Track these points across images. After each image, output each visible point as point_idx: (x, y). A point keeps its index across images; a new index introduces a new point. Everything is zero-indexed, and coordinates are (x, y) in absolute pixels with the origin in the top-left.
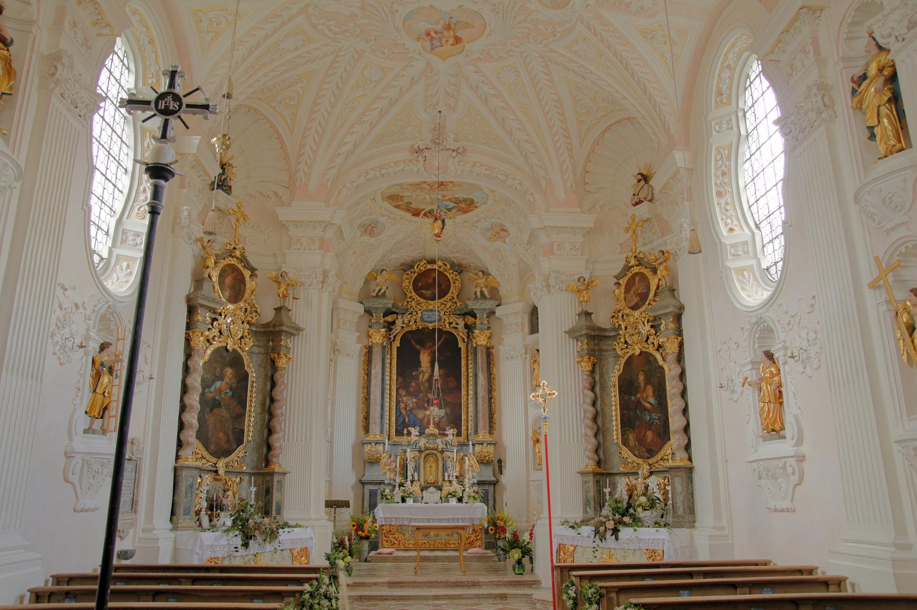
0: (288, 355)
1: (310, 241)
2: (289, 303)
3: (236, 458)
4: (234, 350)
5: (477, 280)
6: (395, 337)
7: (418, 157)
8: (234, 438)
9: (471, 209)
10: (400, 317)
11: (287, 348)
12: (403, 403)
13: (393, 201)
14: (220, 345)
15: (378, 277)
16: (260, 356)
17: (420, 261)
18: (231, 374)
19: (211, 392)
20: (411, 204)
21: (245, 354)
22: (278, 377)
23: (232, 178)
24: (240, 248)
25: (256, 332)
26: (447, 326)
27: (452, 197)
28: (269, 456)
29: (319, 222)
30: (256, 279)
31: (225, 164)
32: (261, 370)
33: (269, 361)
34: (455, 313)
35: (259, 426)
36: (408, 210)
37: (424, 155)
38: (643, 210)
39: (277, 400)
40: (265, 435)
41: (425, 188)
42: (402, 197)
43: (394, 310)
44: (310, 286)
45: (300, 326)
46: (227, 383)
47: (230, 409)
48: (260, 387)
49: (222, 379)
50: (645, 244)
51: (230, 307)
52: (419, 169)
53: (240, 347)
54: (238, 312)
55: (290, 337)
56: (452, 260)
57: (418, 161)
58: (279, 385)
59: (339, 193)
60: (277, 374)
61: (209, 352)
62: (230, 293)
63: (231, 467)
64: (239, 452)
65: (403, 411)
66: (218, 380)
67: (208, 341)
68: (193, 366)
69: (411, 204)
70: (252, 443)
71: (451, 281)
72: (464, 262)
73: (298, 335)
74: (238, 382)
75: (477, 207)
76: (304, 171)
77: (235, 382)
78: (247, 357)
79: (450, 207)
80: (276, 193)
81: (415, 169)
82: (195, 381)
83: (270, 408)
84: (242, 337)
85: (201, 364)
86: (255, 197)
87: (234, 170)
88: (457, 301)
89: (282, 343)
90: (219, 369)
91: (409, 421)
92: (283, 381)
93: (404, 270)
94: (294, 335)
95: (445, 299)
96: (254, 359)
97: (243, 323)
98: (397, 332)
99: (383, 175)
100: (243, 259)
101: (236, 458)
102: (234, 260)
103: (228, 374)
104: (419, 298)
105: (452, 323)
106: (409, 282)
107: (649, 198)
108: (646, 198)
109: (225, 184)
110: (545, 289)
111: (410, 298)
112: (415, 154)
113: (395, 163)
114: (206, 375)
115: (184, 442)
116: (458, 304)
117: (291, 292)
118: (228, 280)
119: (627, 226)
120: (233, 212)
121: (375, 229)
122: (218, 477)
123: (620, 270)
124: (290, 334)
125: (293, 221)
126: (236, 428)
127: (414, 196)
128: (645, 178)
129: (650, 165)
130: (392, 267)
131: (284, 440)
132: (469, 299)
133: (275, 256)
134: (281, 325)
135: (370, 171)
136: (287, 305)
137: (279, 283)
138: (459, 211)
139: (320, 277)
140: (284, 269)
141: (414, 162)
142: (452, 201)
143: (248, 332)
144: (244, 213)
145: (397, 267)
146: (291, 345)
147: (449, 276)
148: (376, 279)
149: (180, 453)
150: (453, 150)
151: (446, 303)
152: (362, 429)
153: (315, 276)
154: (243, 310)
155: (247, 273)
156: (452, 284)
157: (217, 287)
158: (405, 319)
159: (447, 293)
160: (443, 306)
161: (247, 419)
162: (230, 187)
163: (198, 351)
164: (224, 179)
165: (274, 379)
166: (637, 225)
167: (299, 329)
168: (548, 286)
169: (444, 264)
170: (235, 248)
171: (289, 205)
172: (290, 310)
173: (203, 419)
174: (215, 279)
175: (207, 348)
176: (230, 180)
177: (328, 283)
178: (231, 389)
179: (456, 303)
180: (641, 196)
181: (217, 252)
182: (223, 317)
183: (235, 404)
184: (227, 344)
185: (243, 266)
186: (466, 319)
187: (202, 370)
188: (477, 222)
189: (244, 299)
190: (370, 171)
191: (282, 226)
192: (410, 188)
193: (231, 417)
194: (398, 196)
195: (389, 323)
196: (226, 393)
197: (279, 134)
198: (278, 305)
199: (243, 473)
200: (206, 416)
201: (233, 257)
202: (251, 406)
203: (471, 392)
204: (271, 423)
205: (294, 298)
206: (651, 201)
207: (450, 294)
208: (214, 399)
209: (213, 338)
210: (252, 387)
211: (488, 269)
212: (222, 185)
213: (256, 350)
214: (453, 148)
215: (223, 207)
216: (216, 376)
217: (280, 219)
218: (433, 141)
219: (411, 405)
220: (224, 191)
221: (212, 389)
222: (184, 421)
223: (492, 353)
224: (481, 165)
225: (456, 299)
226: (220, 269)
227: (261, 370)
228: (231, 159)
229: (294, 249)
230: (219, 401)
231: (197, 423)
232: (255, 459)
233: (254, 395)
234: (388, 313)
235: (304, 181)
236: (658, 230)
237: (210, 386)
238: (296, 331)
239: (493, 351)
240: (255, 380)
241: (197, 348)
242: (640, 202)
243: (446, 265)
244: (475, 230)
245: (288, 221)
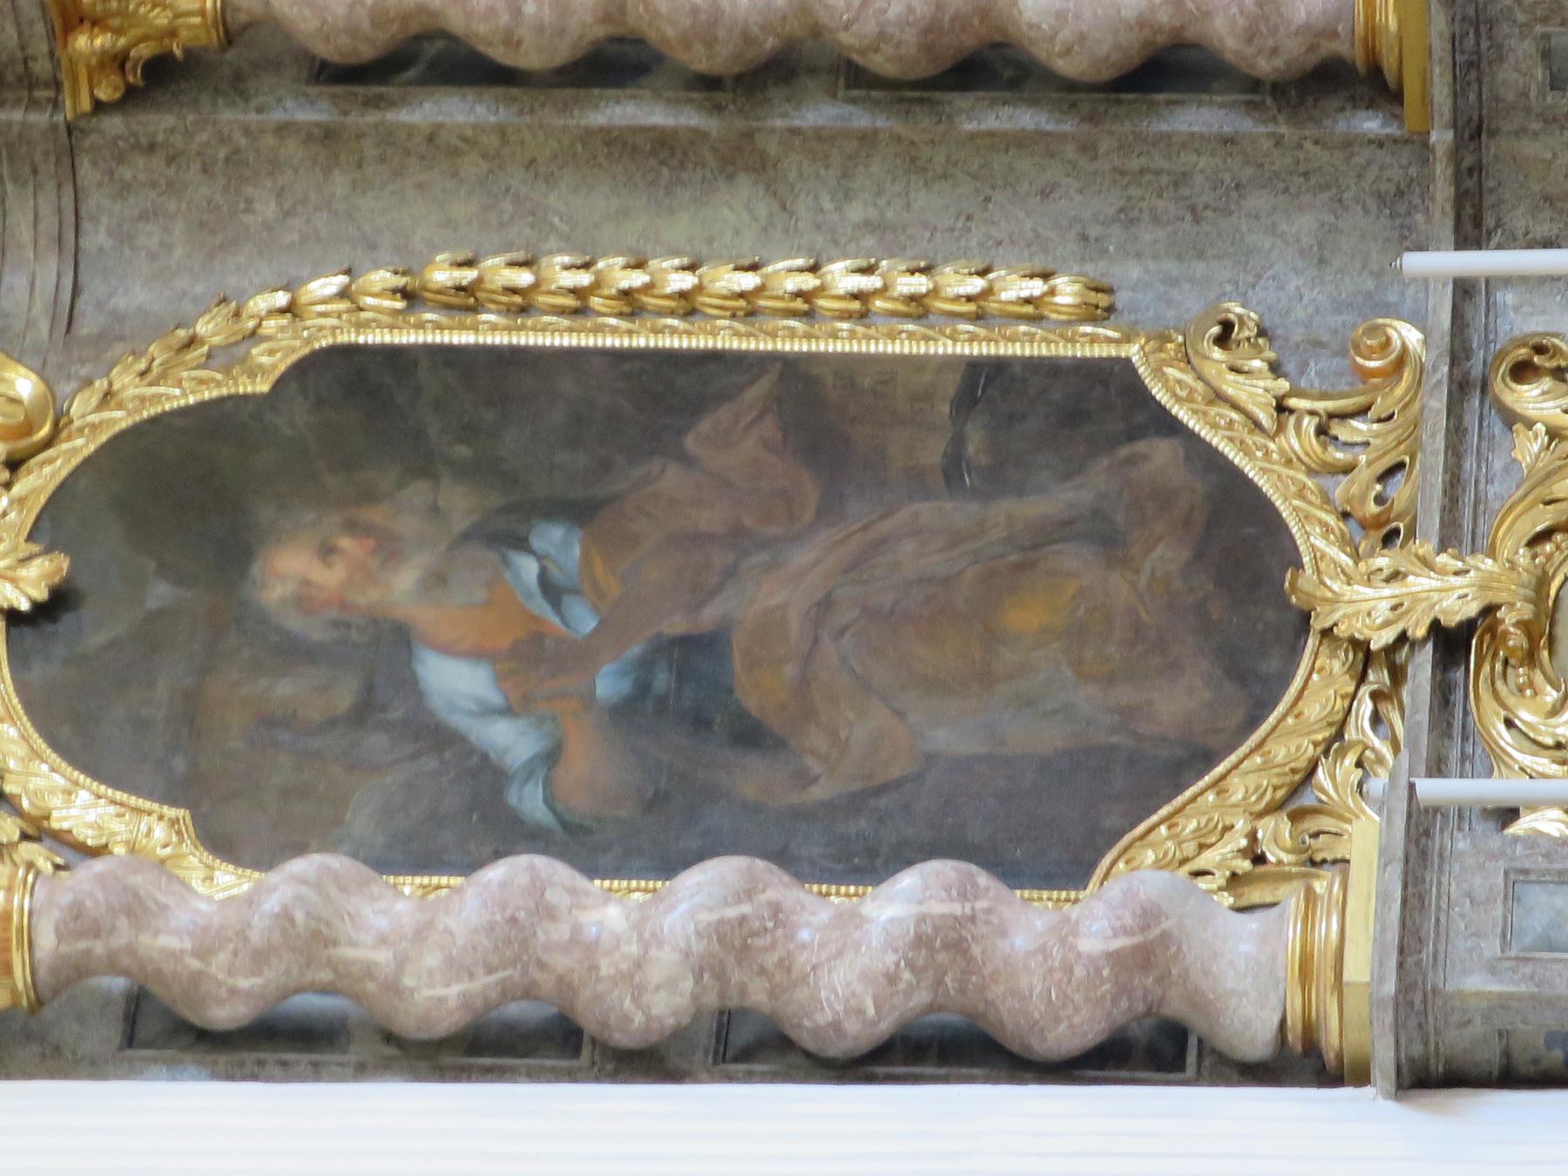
3: (1300, 439)
8: (1071, 472)
16: (97, 238)
18: (327, 552)
19: (552, 757)
21: (81, 407)
33: (160, 122)
35: (921, 199)
40: (1026, 118)
46: (437, 580)
47: (737, 537)
48: (462, 208)
63: (1400, 490)
66: (410, 686)
68: (260, 958)
70: (1127, 274)
74: (424, 465)
77: (417, 493)
78: (125, 381)
83: (708, 84)
85: (230, 881)
90: (284, 689)
101: (1300, 439)
103: (328, 577)
114: (361, 820)
115: (1122, 1012)
122: (1508, 618)
126: (953, 469)
161: (843, 342)
163: (78, 922)
165: (367, 53)
173: (861, 825)
183: (672, 479)
187: (299, 866)
193: (831, 508)
196: (551, 590)
199: (1459, 353)
200: (818, 793)
204: (881, 63)
208: (625, 712)
210: (466, 300)
216: (364, 712)
222: (885, 1027)
230: (645, 666)
231: (908, 880)
232: (1305, 224)
233: (563, 275)
240: (382, 278)
241: (46, 941)
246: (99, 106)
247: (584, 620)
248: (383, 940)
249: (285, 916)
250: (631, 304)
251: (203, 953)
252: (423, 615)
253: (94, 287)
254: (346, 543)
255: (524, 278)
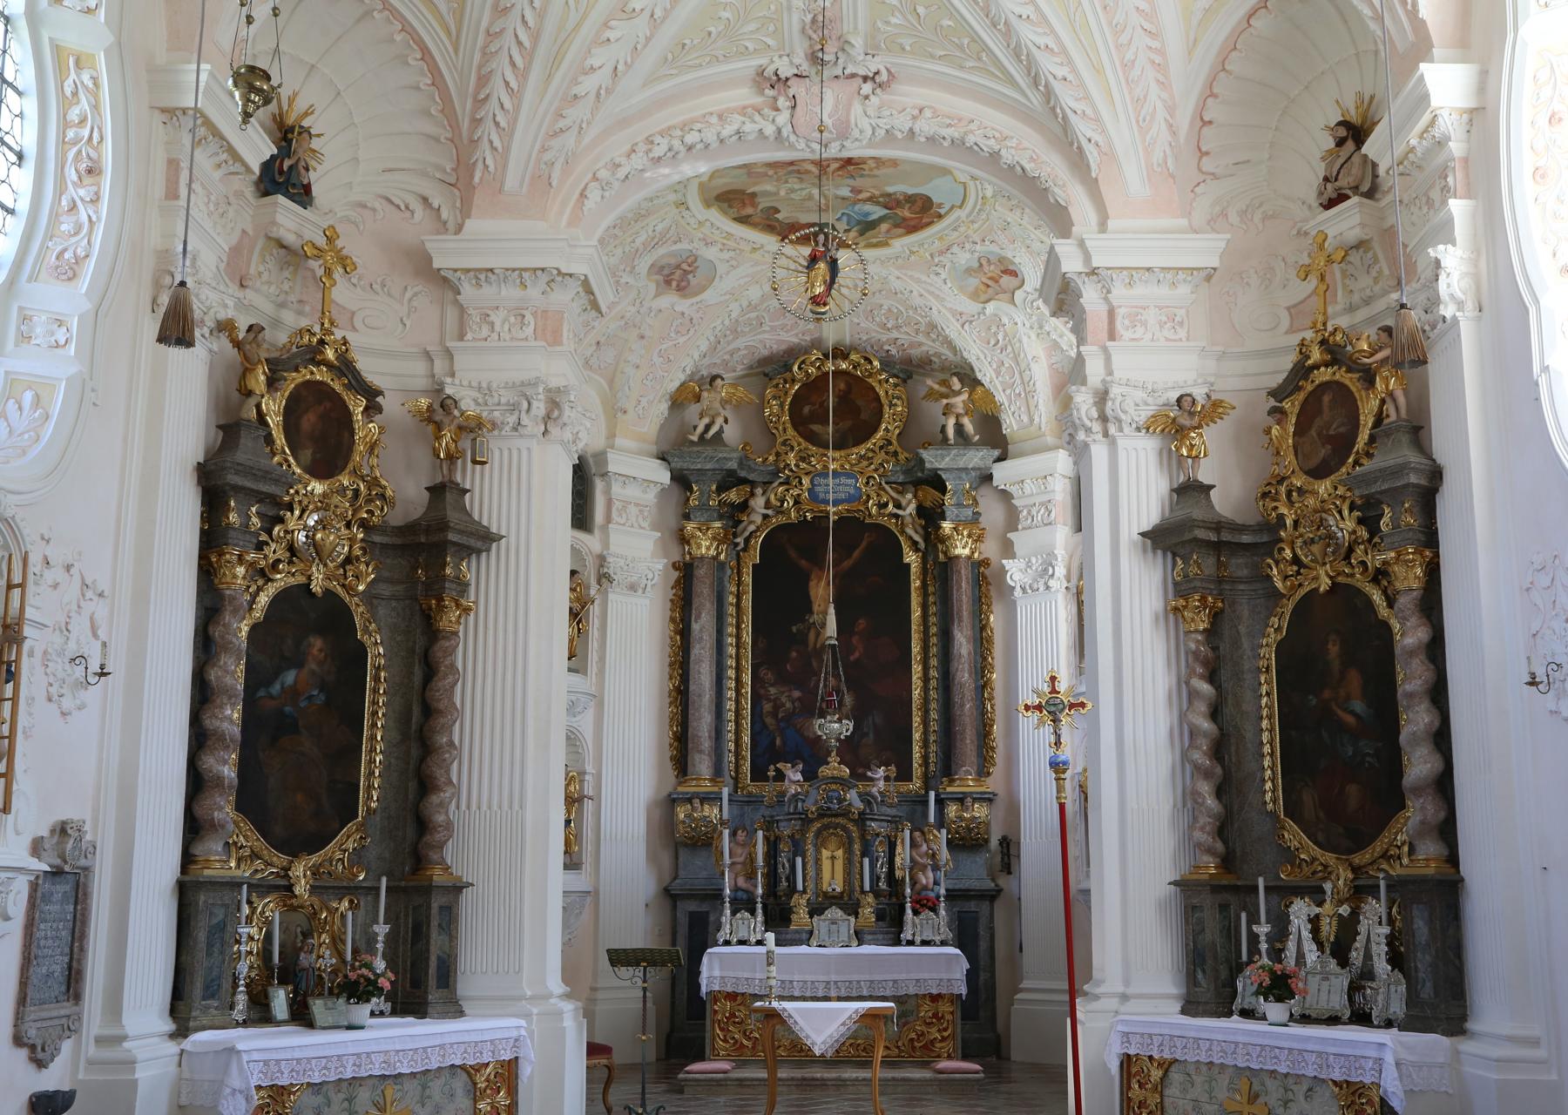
0: (463, 602)
1: (512, 319)
2: (466, 476)
4: (328, 593)
5: (947, 397)
6: (747, 540)
7: (775, 99)
9: (925, 220)
10: (759, 491)
11: (459, 584)
12: (769, 700)
13: (730, 206)
14: (292, 581)
15: (705, 394)
17: (807, 351)
18: (321, 650)
19: (271, 697)
20: (778, 211)
22: (440, 654)
23: (312, 163)
24: (335, 342)
25: (384, 546)
26: (874, 510)
27: (877, 193)
28: (420, 846)
29: (535, 270)
30: (377, 417)
31: (292, 129)
32: (399, 638)
34: (893, 479)
36: (769, 226)
37: (791, 92)
38: (1347, 221)
39: (439, 712)
41: (807, 172)
42: (754, 195)
43: (743, 474)
44: (515, 429)
45: (494, 530)
46: (313, 673)
49: (299, 664)
50: (1351, 309)
51: (318, 487)
52: (779, 131)
53: (343, 586)
54: (337, 499)
55: (469, 556)
56: (886, 347)
57: (777, 110)
58: (441, 674)
59: (583, 195)
60: (436, 648)
61: (263, 599)
62: (314, 453)
64: (347, 841)
65: (769, 720)
66: (289, 668)
67: (262, 573)
69: (778, 211)
71: (884, 400)
72: (915, 353)
73: (488, 550)
75: (940, 216)
76: (491, 142)
79: (874, 217)
80: (425, 200)
81: (770, 130)
82: (232, 673)
83: (421, 730)
84: (348, 560)
86: (374, 210)
87: (315, 144)
88: (899, 450)
89: (448, 571)
91: (784, 742)
92: (453, 666)
93: (766, 375)
94: (479, 552)
95: (869, 445)
96: (381, 611)
97: (348, 526)
98: (752, 528)
99: (690, 148)
100: (345, 367)
102: (321, 371)
103: (315, 651)
104: (804, 444)
105: (886, 505)
106: (782, 406)
107: (1365, 187)
108: (1357, 187)
109: (293, 180)
110: (1096, 427)
111: (784, 443)
112: (770, 92)
113: (720, 117)
116: (901, 457)
117: (465, 444)
118: (309, 421)
119: (1307, 261)
120: (315, 252)
121: (690, 276)
123: (1285, 374)
124: (467, 551)
125: (468, 271)
127: (782, 193)
128: (1354, 132)
129: (1372, 98)
130: (740, 367)
131: (458, 808)
132: (927, 445)
133: (428, 356)
134: (443, 526)
135: (658, 139)
136: (459, 479)
137: (439, 427)
138: (896, 226)
139: (540, 408)
140: (449, 391)
141: (766, 111)
142: (878, 203)
143: (362, 548)
144: (345, 252)
145: (751, 367)
146: (471, 577)
147: (877, 389)
148: (698, 399)
149: (198, 850)
150: (865, 79)
151: (870, 455)
152: (669, 765)
153: (525, 405)
154: (350, 494)
155: (357, 406)
156: (886, 408)
157: (280, 439)
158: (772, 497)
159: (876, 429)
160: (865, 463)
162: (307, 189)
164: (291, 167)
166: (1330, 261)
167: (487, 538)
168: (1103, 419)
169: (866, 359)
170: (322, 342)
171: (459, 229)
172: (468, 491)
174: (274, 421)
175: (259, 589)
176: (307, 169)
177: (560, 422)
178: (323, 687)
179: (895, 454)
180: (1344, 182)
181: (276, 355)
182: (297, 513)
184: (309, 578)
185: (344, 385)
186: (920, 494)
188: (941, 253)
189: (350, 466)
190: (658, 139)
191: (444, 283)
192: (771, 173)
194: (742, 192)
195: (732, 505)
196: (310, 697)
197: (425, 50)
198: (439, 480)
201: (318, 364)
202: (374, 725)
203: (933, 673)
205: (475, 462)
206: (1371, 194)
207: (880, 434)
209: (274, 566)
210: (377, 679)
211: (972, 369)
212: (288, 180)
213: (385, 590)
214: (862, 72)
215: (290, 239)
217: (436, 265)
218: (816, 59)
219: (788, 705)
220: (291, 198)
221: (276, 688)
223: (985, 577)
224: (936, 114)
225: (895, 446)
226: (287, 394)
227: (399, 638)
228: (306, 114)
229: (474, 339)
234: (729, 480)
235: (491, 168)
236: (1386, 272)
237: (269, 683)
238: (483, 539)
239: (987, 572)
242: (1341, 198)
243: (871, 363)
244: (938, 274)
245: (455, 270)
246: (421, 605)
247: (303, 704)
248: (225, 663)
249: (231, 643)
250: (375, 713)
251: (224, 625)
252: (305, 671)
253: (383, 603)
254: (323, 654)
255: (381, 692)
